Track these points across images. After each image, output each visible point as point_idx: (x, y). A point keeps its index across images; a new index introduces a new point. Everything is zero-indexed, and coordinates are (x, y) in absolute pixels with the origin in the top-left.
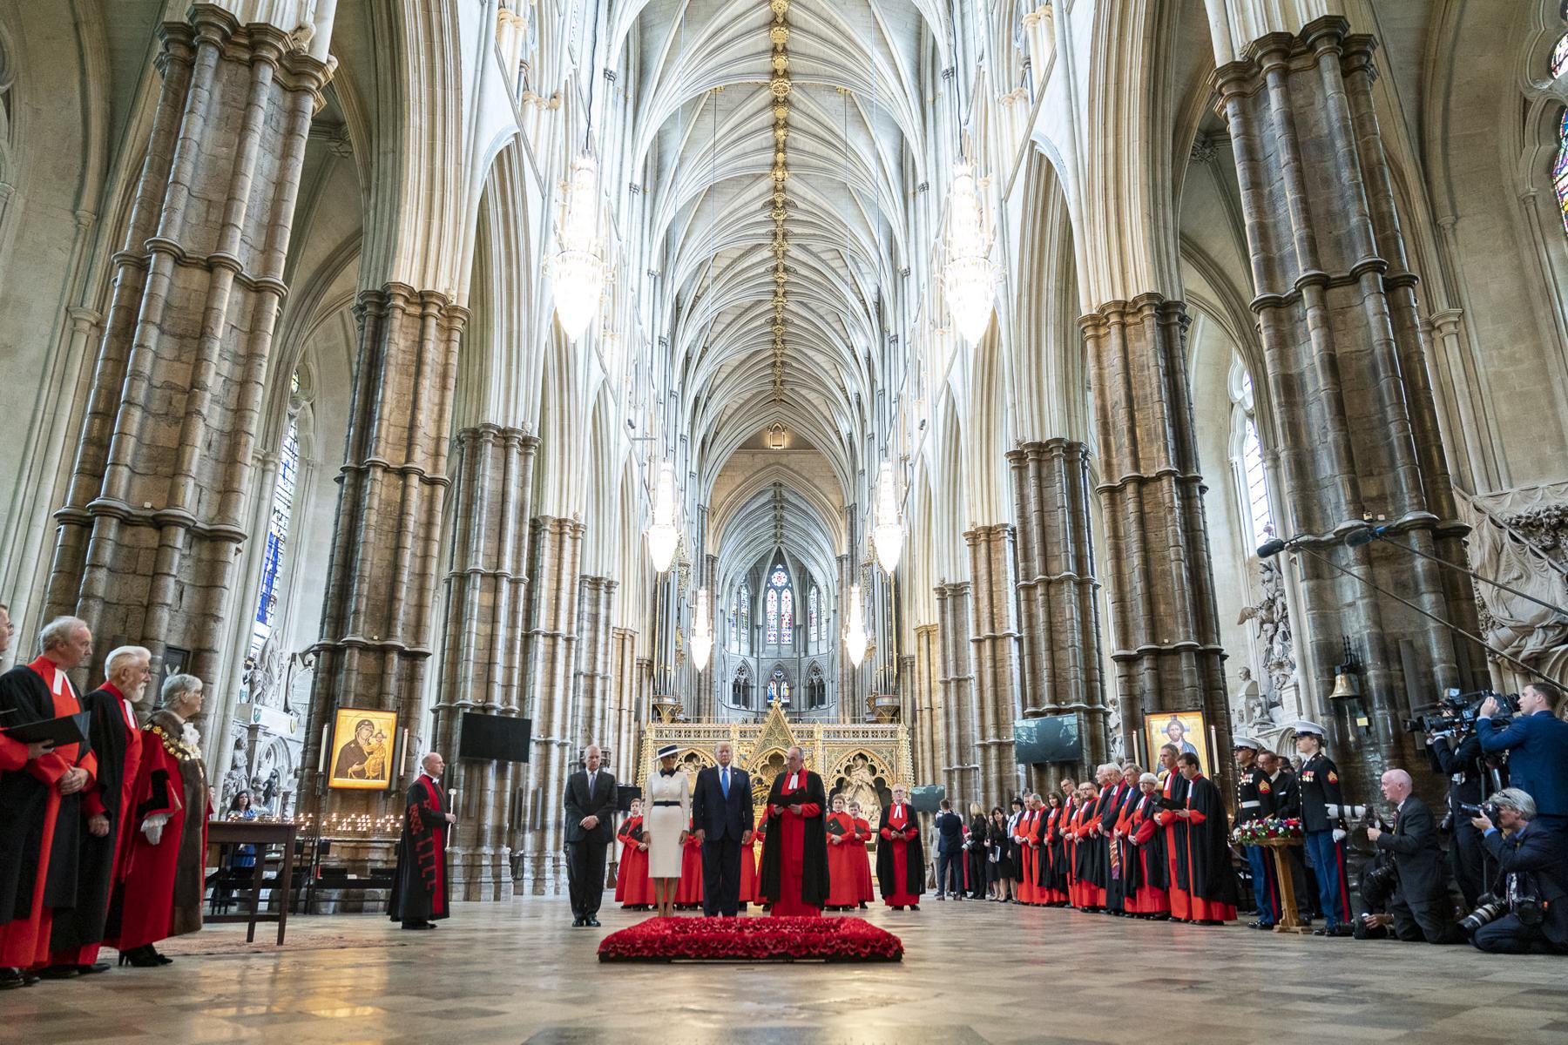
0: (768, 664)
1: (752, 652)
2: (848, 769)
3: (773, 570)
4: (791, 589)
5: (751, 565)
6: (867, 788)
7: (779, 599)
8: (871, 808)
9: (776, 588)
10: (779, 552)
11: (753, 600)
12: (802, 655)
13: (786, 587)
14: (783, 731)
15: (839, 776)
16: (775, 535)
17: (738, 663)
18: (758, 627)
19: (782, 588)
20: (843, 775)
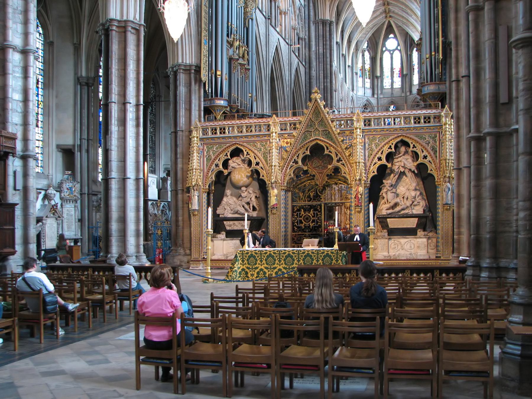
0: (384, 101)
1: (373, 94)
2: (390, 157)
3: (386, 38)
4: (400, 51)
5: (369, 35)
6: (409, 174)
7: (392, 58)
8: (413, 193)
9: (389, 51)
10: (390, 26)
11: (373, 60)
12: (408, 94)
13: (397, 49)
14: (323, 122)
15: (380, 163)
16: (385, 12)
17: (363, 102)
18: (377, 77)
19: (394, 51)
20: (384, 161)
